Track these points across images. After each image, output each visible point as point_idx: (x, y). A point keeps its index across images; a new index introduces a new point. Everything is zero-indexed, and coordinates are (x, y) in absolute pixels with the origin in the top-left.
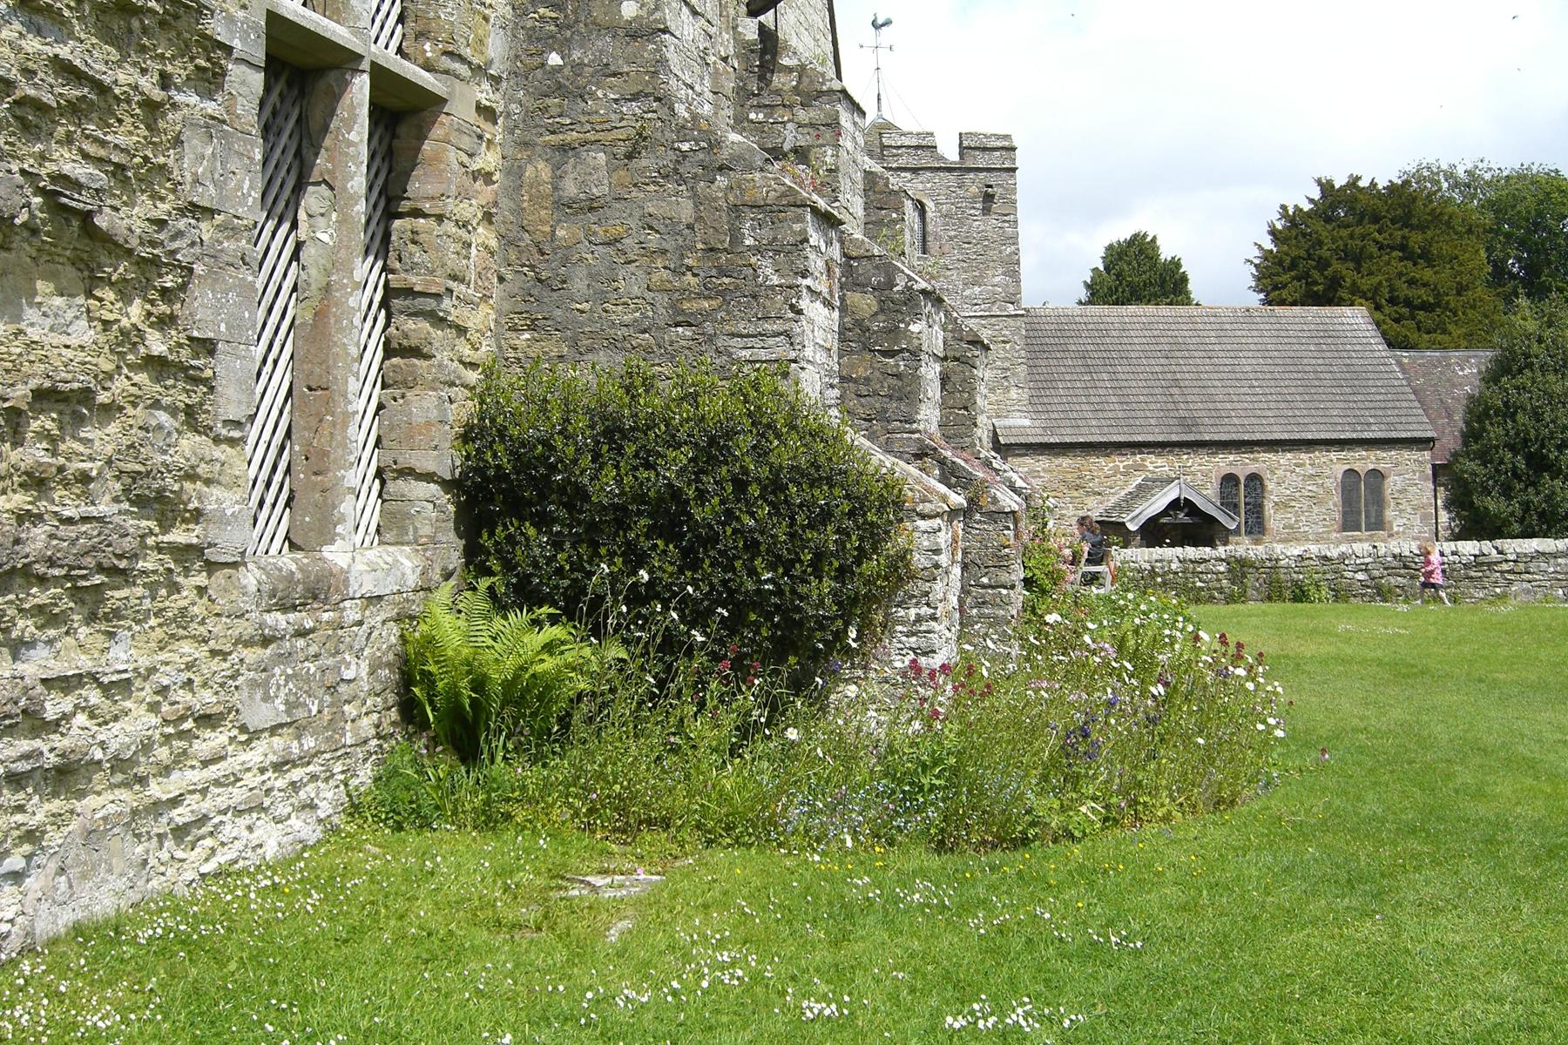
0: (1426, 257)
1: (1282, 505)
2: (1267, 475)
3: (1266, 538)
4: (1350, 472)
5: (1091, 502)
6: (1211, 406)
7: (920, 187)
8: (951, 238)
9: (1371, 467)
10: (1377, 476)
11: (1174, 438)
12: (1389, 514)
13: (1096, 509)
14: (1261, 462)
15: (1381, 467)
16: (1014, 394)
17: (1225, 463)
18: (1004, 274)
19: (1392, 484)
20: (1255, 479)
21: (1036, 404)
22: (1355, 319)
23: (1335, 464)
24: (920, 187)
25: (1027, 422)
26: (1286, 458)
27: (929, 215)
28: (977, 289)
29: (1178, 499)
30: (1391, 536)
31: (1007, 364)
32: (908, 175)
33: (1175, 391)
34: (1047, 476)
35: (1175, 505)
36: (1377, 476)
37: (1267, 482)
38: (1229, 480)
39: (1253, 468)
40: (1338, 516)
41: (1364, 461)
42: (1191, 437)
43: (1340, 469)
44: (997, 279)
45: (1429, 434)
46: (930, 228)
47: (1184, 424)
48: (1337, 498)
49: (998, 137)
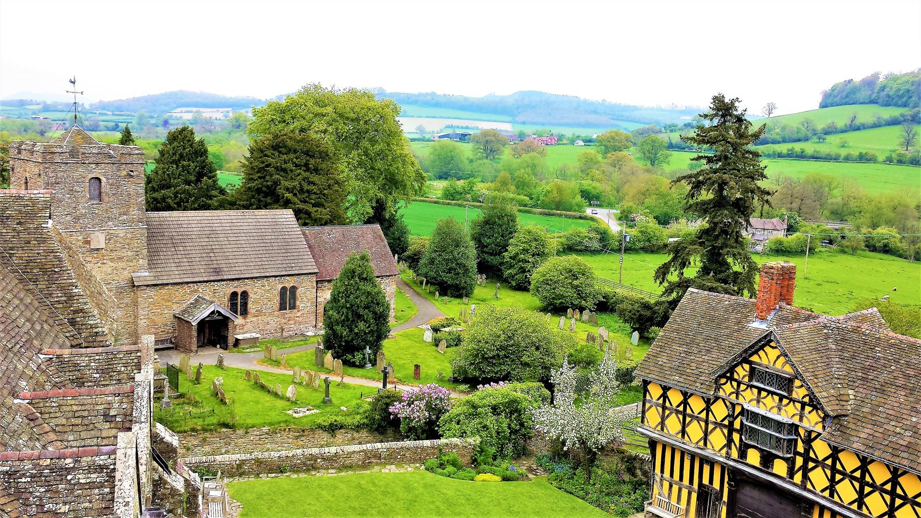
0: (316, 171)
4: (284, 288)
5: (175, 307)
6: (227, 261)
10: (294, 289)
11: (212, 278)
12: (298, 303)
13: (177, 309)
14: (248, 286)
19: (299, 292)
20: (245, 294)
21: (151, 265)
22: (287, 215)
25: (147, 274)
27: (103, 184)
28: (125, 217)
32: (94, 166)
33: (212, 255)
35: (213, 313)
36: (294, 289)
38: (234, 294)
39: (243, 289)
40: (278, 305)
43: (280, 286)
45: (316, 271)
46: (103, 190)
48: (278, 298)
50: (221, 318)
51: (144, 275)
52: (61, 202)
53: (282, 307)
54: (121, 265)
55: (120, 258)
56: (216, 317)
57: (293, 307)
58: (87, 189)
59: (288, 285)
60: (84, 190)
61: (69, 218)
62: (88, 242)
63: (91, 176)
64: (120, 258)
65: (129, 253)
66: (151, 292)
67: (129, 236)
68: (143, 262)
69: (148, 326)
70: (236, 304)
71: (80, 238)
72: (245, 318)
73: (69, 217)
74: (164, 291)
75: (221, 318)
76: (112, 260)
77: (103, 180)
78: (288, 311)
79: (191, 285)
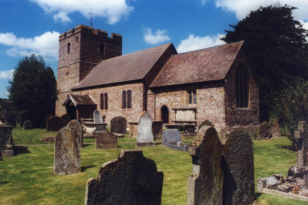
1: (111, 101)
2: (108, 94)
3: (108, 110)
4: (124, 91)
9: (128, 89)
10: (129, 92)
12: (132, 103)
15: (130, 89)
17: (100, 91)
19: (133, 94)
23: (120, 89)
26: (112, 88)
30: (133, 110)
36: (129, 92)
37: (108, 95)
41: (127, 87)
48: (121, 99)
53: (124, 107)
57: (130, 107)
59: (126, 90)
78: (126, 109)
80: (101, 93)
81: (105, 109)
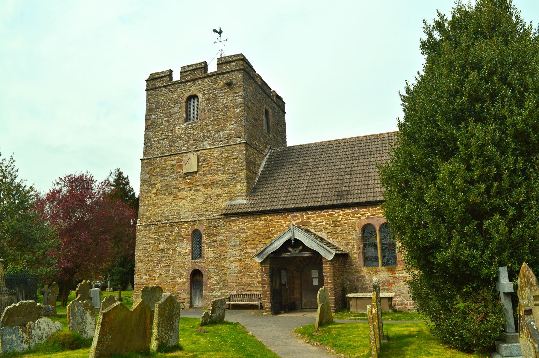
7: (196, 88)
8: (209, 110)
16: (239, 186)
18: (236, 123)
21: (252, 191)
24: (196, 88)
25: (245, 202)
28: (221, 133)
29: (289, 241)
31: (235, 171)
32: (190, 84)
34: (249, 232)
35: (288, 243)
42: (341, 202)
44: (232, 126)
47: (340, 195)
49: (234, 56)
50: (308, 254)
51: (242, 201)
52: (160, 126)
54: (217, 191)
55: (215, 184)
56: (293, 252)
58: (184, 110)
60: (178, 110)
61: (165, 142)
62: (181, 166)
63: (187, 94)
64: (215, 184)
65: (225, 177)
66: (239, 224)
67: (225, 155)
68: (241, 187)
69: (240, 272)
70: (375, 246)
71: (174, 162)
72: (392, 271)
73: (165, 141)
74: (260, 222)
75: (308, 254)
76: (206, 186)
77: (200, 96)
79: (298, 214)
80: (364, 223)
81: (384, 264)
